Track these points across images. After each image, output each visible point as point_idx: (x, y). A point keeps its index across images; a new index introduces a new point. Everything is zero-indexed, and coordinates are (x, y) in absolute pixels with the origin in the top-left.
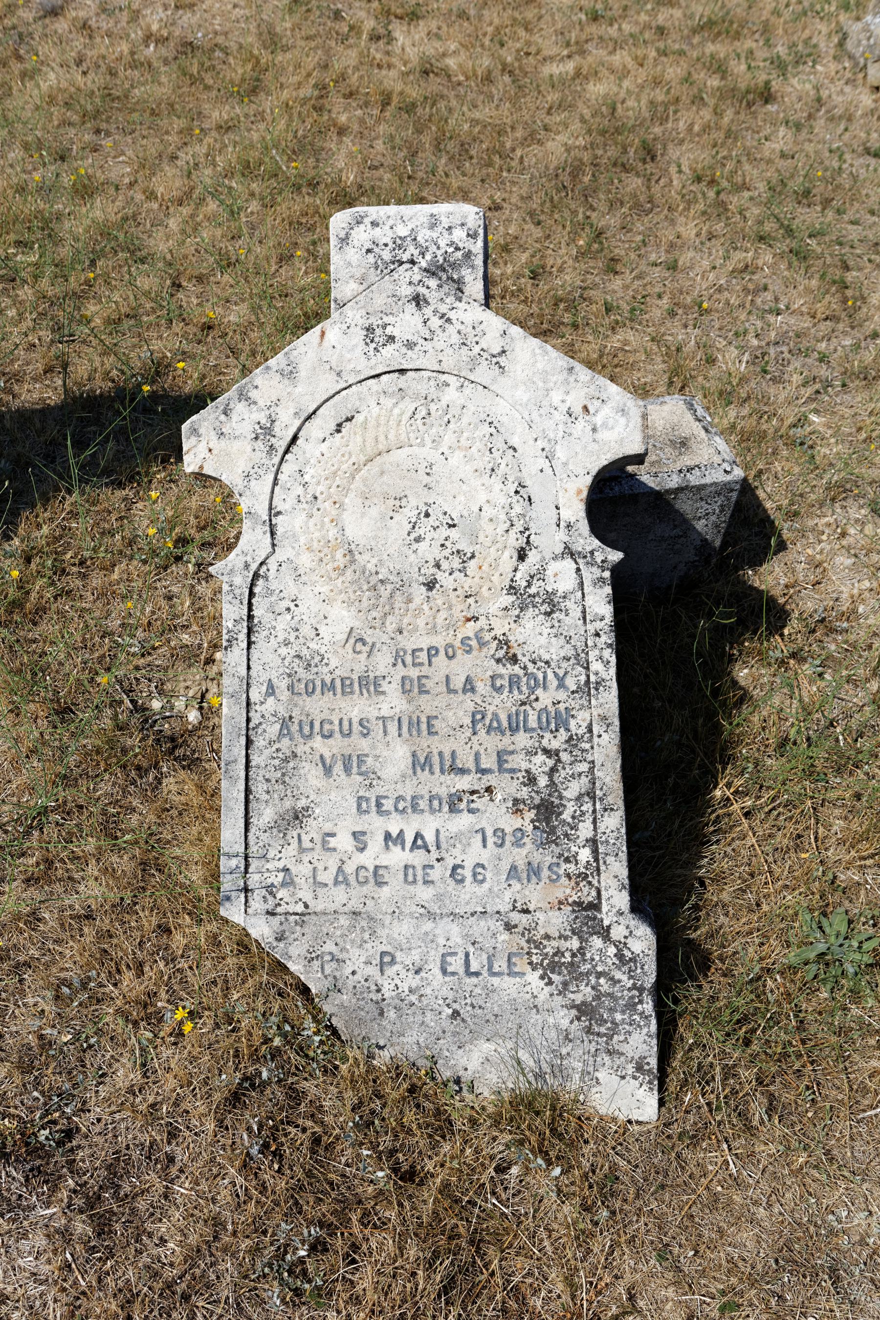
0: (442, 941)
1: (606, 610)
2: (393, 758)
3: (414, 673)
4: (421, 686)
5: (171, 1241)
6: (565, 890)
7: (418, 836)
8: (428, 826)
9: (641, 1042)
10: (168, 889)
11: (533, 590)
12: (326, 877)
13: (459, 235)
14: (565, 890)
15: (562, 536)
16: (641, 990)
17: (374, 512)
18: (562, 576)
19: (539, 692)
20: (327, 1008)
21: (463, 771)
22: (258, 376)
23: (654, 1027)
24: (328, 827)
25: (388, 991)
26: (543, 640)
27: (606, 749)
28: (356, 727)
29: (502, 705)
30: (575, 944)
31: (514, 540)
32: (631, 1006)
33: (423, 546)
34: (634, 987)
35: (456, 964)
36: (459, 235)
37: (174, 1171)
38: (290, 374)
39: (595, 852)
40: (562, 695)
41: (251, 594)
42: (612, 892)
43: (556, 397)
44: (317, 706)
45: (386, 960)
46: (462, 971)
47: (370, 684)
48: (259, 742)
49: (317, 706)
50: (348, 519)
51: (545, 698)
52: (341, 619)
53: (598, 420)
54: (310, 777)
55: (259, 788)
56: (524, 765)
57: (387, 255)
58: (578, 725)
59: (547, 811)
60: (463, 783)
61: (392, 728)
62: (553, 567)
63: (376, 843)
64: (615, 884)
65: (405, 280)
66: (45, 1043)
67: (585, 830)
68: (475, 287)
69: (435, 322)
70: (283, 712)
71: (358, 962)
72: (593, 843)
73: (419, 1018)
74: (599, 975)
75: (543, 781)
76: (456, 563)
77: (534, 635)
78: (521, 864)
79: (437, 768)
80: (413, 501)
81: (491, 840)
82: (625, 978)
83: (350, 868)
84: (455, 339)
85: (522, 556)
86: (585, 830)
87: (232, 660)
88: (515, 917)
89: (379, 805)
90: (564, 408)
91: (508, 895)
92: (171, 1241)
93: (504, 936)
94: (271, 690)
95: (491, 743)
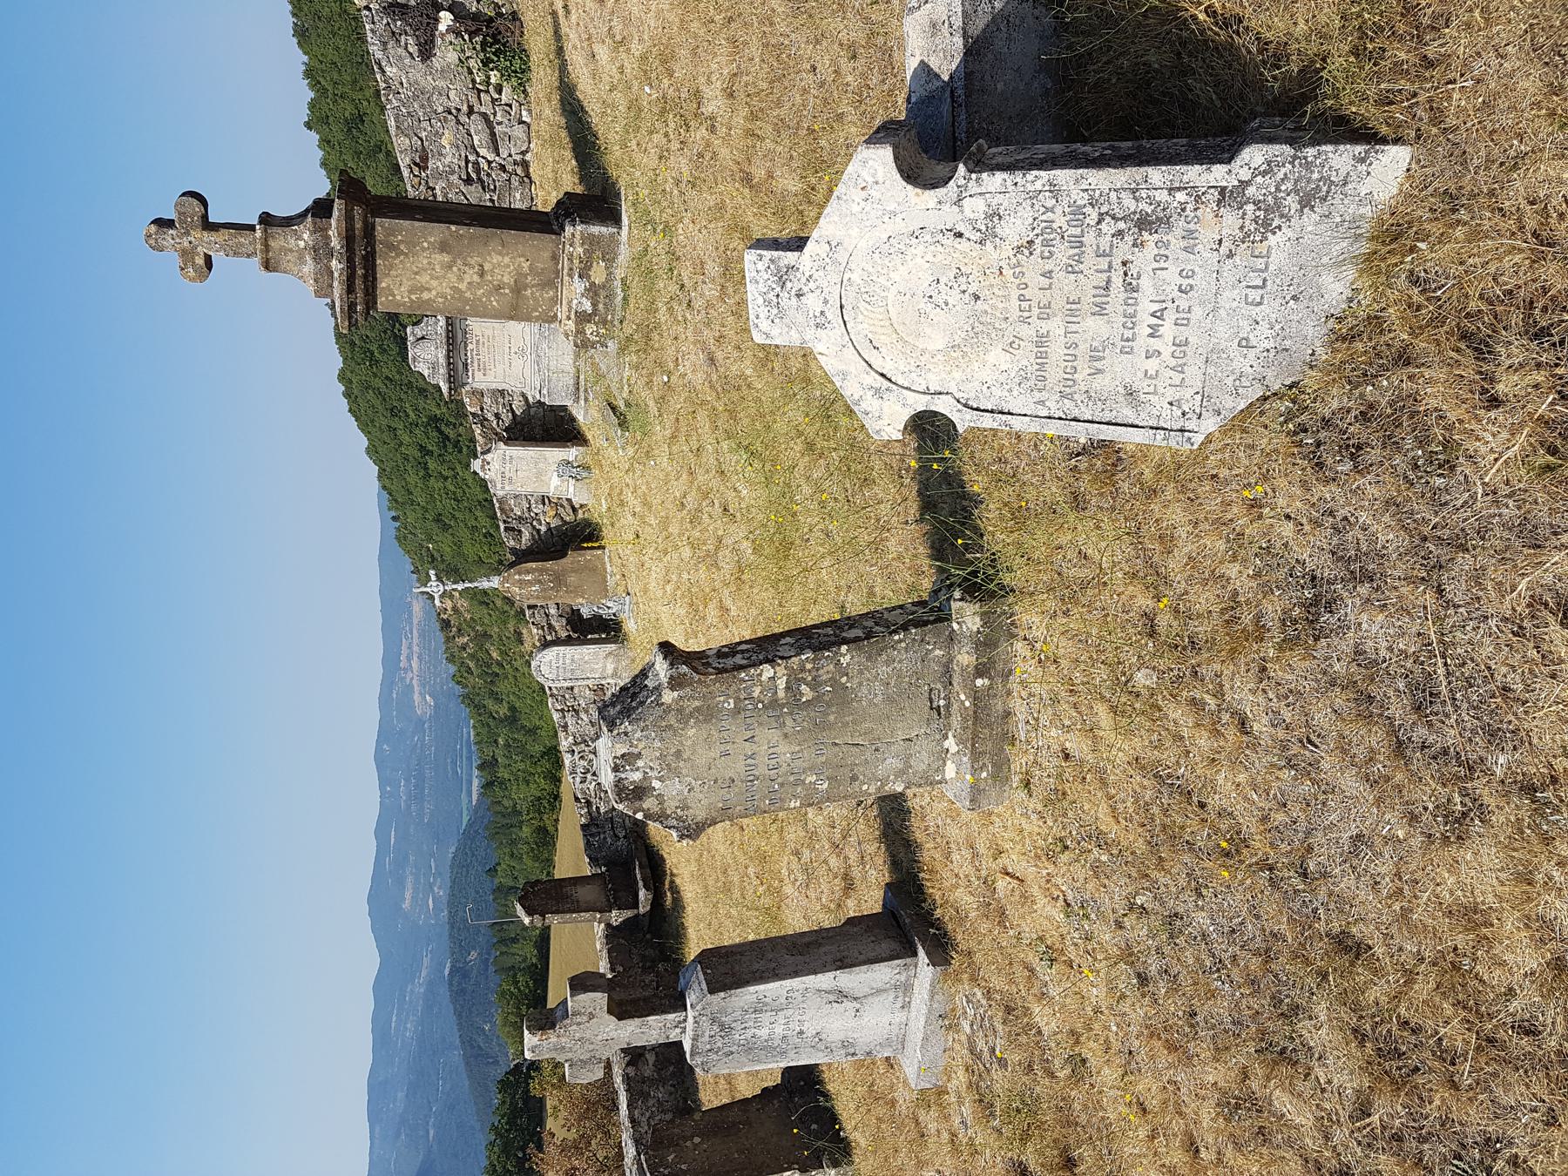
0: (1235, 304)
1: (1000, 176)
2: (1093, 328)
3: (1036, 311)
4: (1045, 307)
5: (1389, 537)
6: (1207, 213)
7: (1153, 315)
8: (1146, 307)
9: (1340, 158)
10: (1182, 473)
11: (983, 228)
12: (1177, 378)
13: (760, 266)
14: (1207, 213)
15: (946, 207)
16: (1295, 157)
17: (928, 331)
18: (975, 207)
19: (1055, 226)
20: (1276, 387)
21: (1109, 281)
22: (846, 393)
23: (1329, 148)
24: (1140, 375)
25: (1270, 344)
26: (1018, 222)
27: (1100, 179)
28: (1070, 351)
29: (1063, 252)
30: (1250, 208)
31: (948, 240)
32: (1308, 166)
33: (951, 301)
34: (1292, 162)
35: (1255, 295)
36: (760, 266)
37: (1352, 519)
38: (844, 375)
39: (1179, 189)
40: (1059, 210)
41: (977, 409)
42: (1211, 178)
43: (856, 208)
44: (1054, 374)
45: (1245, 344)
46: (1260, 292)
47: (1042, 341)
48: (1076, 413)
49: (1054, 374)
50: (932, 347)
51: (1060, 221)
52: (996, 356)
53: (870, 180)
54: (1102, 383)
55: (1107, 416)
56: (1108, 238)
57: (775, 311)
58: (1082, 199)
59: (1144, 223)
60: (1117, 280)
61: (1073, 327)
62: (968, 213)
63: (1155, 344)
64: (1205, 176)
65: (789, 302)
66: (1258, 575)
67: (1162, 196)
68: (790, 257)
69: (812, 285)
70: (1057, 397)
71: (1245, 363)
72: (1171, 190)
73: (1294, 324)
74: (1278, 189)
75: (1121, 225)
76: (962, 280)
77: (1014, 229)
78: (1183, 244)
79: (1104, 299)
80: (922, 305)
81: (1163, 265)
82: (1283, 170)
83: (1173, 362)
84: (821, 273)
85: (960, 235)
86: (1162, 196)
87: (1017, 424)
88: (1224, 250)
89: (1128, 340)
90: (863, 204)
91: (1206, 255)
92: (1389, 537)
93: (1237, 258)
94: (1042, 403)
95: (1090, 260)
